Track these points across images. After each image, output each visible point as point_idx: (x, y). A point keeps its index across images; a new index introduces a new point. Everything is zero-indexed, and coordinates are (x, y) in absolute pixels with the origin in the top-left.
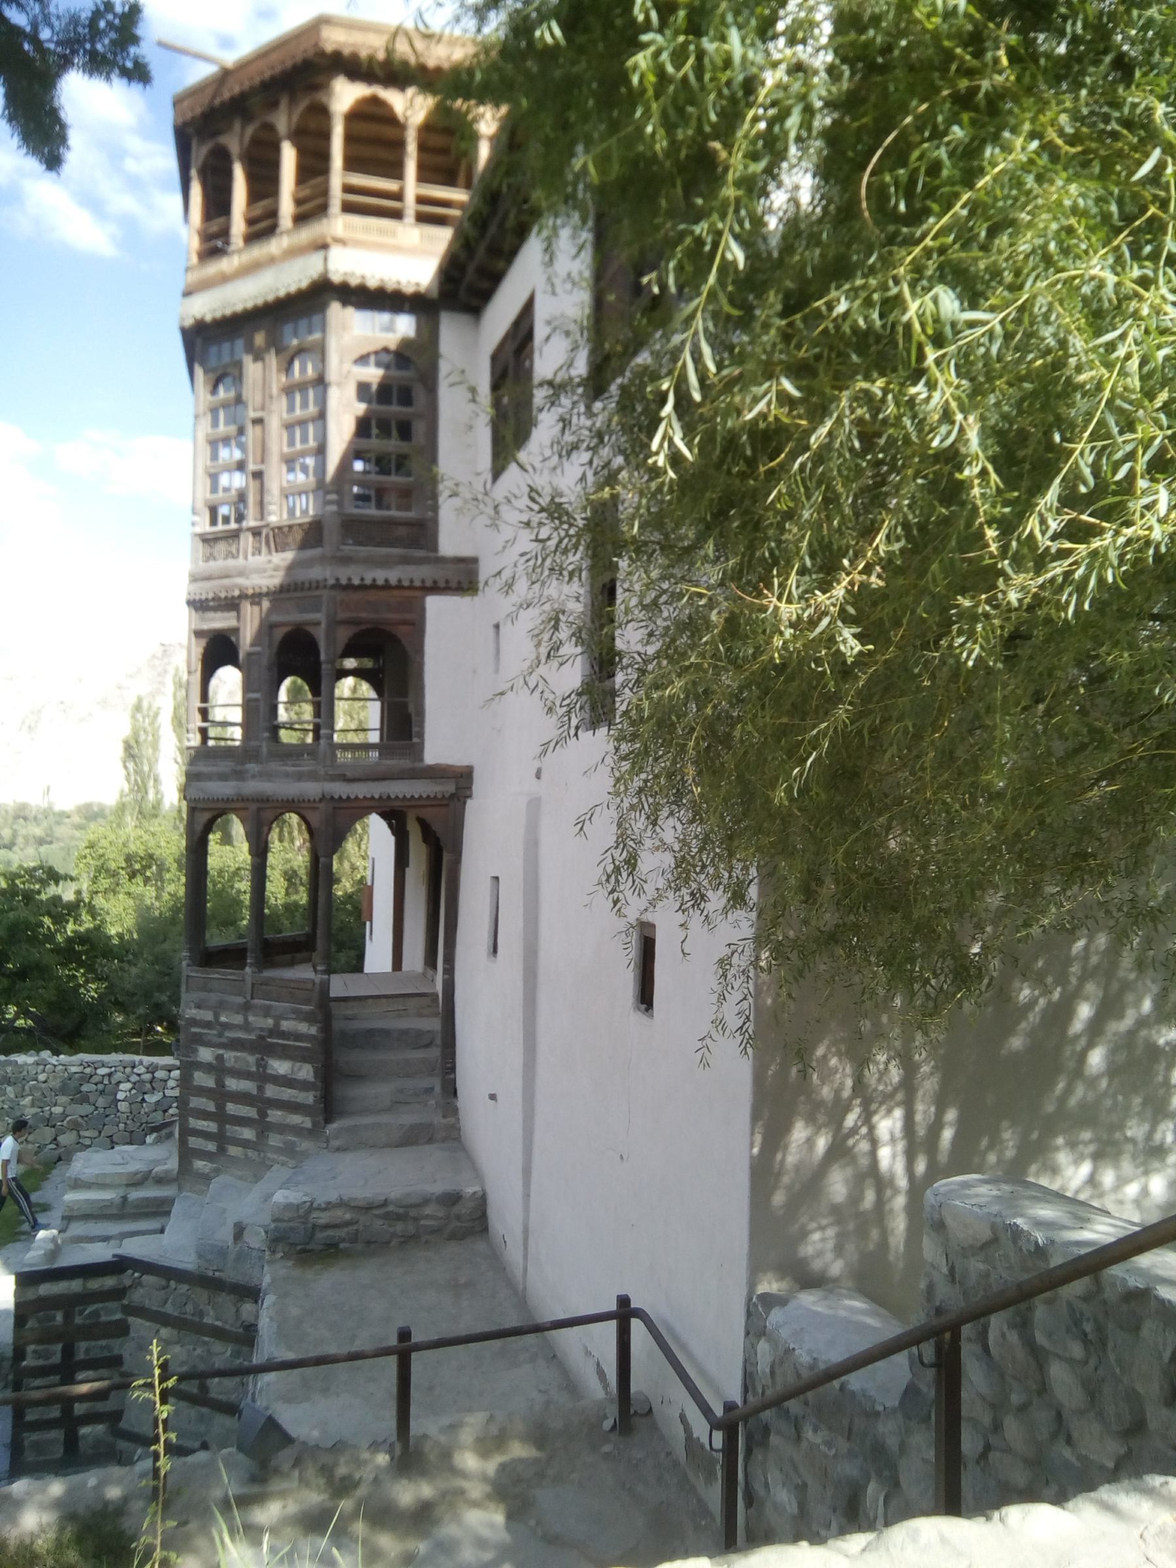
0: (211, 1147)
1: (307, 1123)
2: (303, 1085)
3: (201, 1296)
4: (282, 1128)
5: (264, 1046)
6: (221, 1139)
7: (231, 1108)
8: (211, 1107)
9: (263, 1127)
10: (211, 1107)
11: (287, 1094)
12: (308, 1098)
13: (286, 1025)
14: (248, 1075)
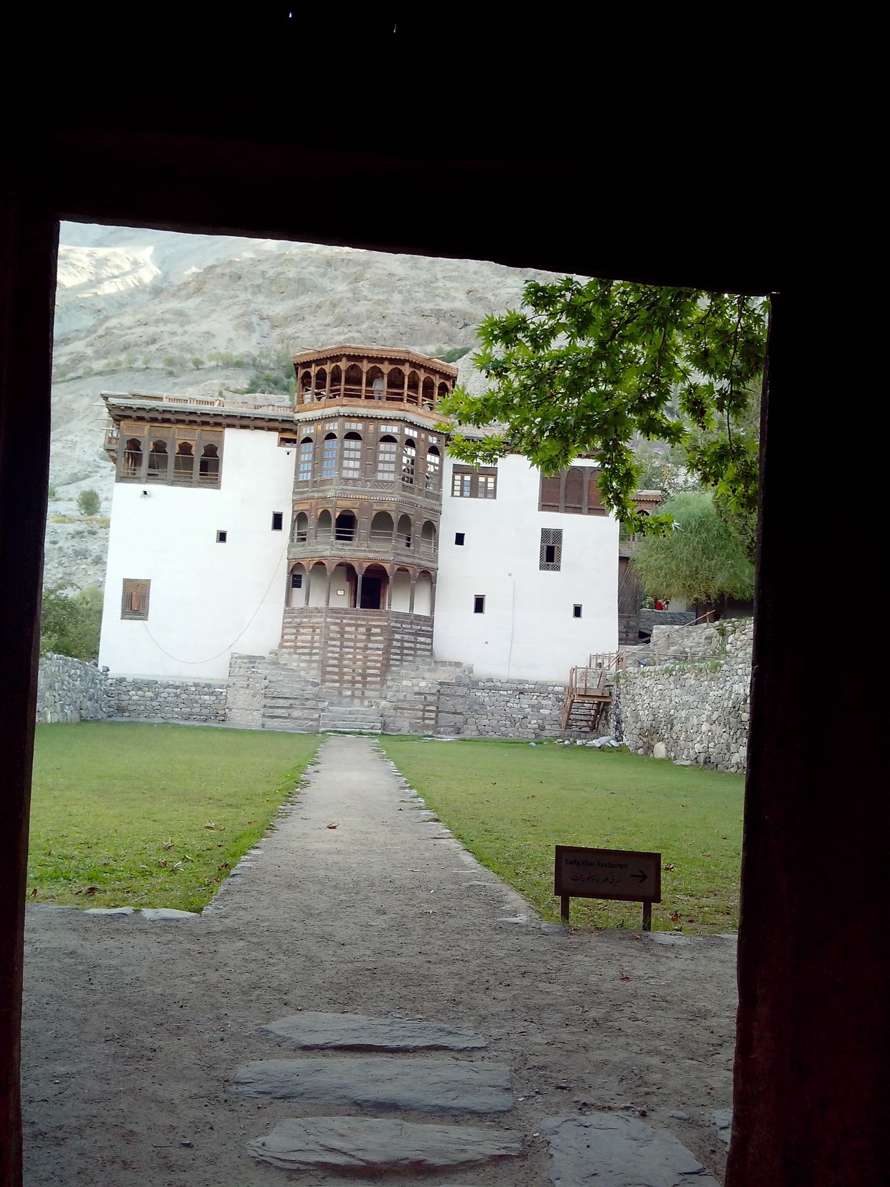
1: (429, 654)
2: (428, 644)
4: (421, 656)
5: (416, 634)
6: (401, 660)
9: (415, 656)
11: (423, 646)
12: (429, 647)
13: (423, 628)
14: (411, 642)
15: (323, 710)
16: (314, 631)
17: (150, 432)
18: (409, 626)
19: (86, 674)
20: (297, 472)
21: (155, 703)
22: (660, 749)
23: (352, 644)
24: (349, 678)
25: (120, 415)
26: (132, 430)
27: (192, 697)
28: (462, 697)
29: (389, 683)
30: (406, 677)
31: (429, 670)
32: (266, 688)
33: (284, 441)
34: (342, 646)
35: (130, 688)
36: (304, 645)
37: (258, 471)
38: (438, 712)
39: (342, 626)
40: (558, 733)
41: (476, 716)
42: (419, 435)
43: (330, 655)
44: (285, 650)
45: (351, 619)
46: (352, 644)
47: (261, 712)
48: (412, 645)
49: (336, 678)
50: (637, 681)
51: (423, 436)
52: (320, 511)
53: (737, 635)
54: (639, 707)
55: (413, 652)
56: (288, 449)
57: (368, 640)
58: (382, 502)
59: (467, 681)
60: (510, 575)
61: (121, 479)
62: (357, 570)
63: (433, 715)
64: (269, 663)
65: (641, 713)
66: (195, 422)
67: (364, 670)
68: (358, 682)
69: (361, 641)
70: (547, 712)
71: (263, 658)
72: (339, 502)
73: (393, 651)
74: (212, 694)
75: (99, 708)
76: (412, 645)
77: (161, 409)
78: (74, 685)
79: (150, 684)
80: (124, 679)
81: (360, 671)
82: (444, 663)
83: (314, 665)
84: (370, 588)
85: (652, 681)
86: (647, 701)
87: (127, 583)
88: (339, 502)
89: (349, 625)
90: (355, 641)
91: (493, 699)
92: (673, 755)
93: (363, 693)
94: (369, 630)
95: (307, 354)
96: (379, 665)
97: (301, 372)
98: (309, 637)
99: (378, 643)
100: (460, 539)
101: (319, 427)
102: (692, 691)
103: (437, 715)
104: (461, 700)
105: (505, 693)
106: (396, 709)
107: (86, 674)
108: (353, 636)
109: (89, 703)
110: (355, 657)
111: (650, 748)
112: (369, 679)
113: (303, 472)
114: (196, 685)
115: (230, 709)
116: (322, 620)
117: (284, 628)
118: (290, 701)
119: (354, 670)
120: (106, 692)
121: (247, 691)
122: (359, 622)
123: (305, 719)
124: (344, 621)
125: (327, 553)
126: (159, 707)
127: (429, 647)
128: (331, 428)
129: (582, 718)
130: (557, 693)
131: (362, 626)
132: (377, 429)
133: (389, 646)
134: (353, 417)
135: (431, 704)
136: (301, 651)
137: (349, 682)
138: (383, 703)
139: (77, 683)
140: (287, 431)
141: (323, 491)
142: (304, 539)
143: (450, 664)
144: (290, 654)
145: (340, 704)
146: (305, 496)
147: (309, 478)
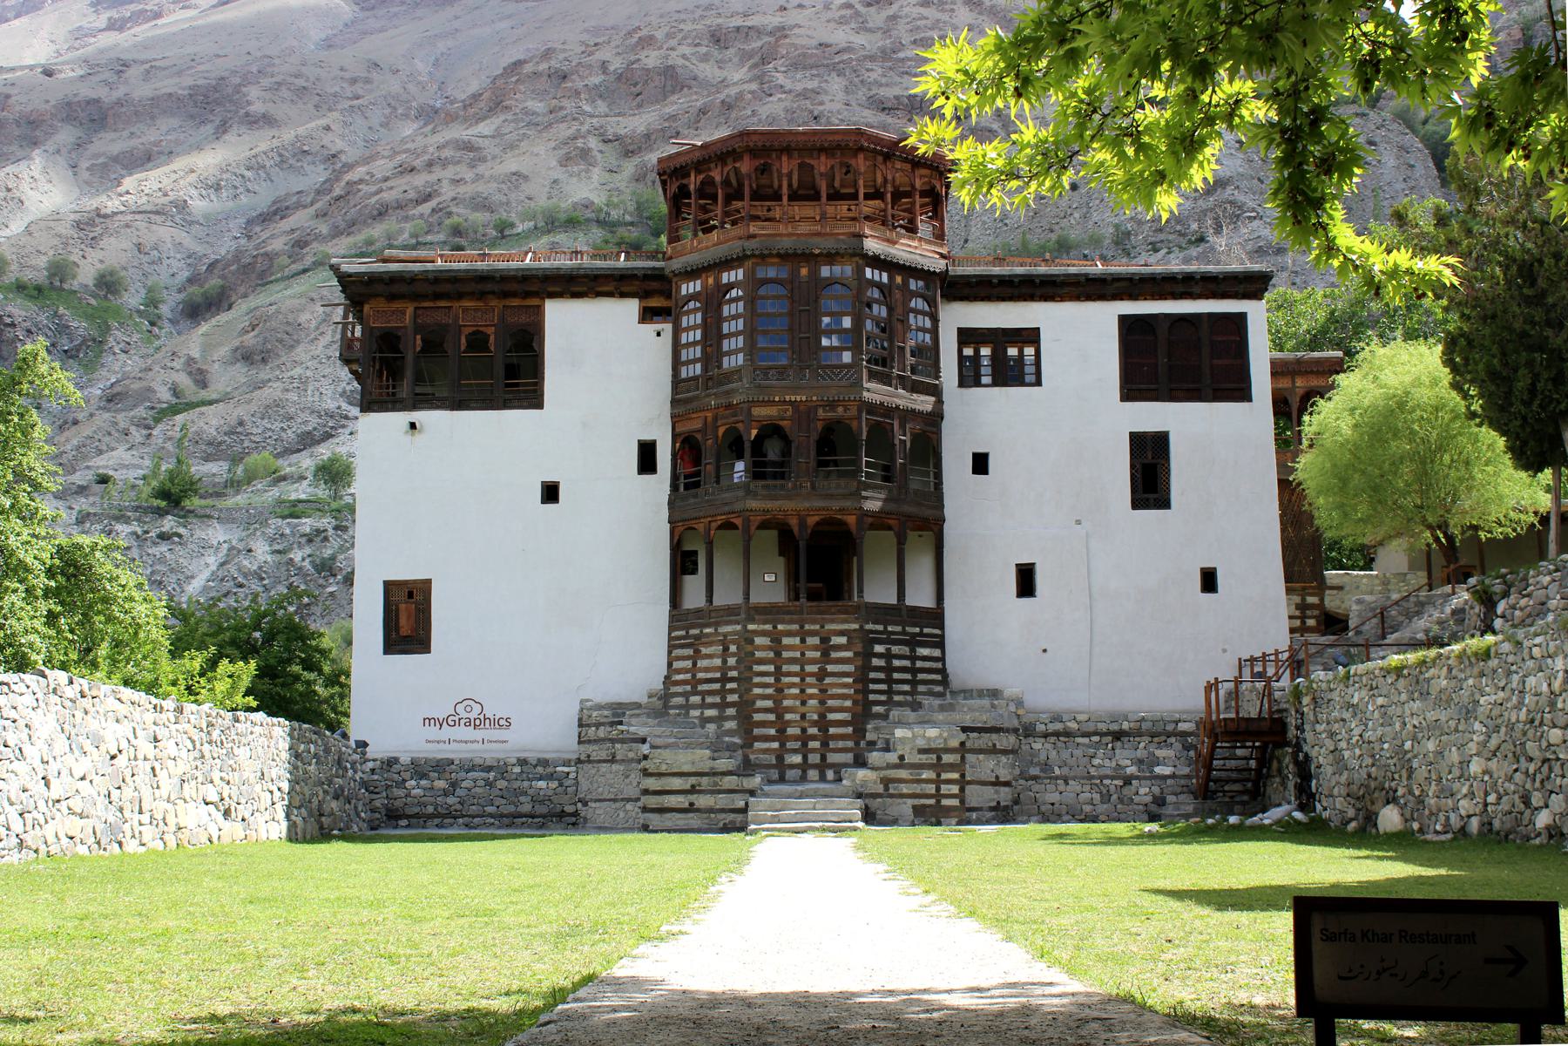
0: (883, 698)
1: (938, 677)
3: (994, 736)
6: (889, 692)
7: (896, 676)
8: (882, 676)
9: (914, 683)
10: (882, 676)
11: (928, 664)
12: (939, 665)
13: (926, 630)
15: (752, 793)
16: (726, 649)
17: (416, 316)
18: (899, 629)
19: (327, 751)
20: (677, 363)
21: (451, 800)
22: (1390, 818)
23: (796, 668)
24: (797, 731)
25: (358, 291)
26: (382, 314)
27: (516, 784)
28: (1005, 752)
29: (870, 736)
30: (901, 723)
31: (942, 708)
32: (646, 757)
33: (647, 315)
34: (778, 674)
35: (407, 775)
36: (710, 675)
37: (608, 369)
38: (963, 783)
39: (776, 639)
40: (1190, 809)
41: (1036, 787)
42: (891, 278)
43: (757, 691)
44: (679, 689)
45: (791, 622)
46: (796, 668)
47: (640, 804)
48: (907, 663)
49: (772, 732)
50: (1335, 696)
51: (899, 279)
52: (721, 431)
53: (1512, 599)
54: (1343, 745)
55: (908, 676)
56: (658, 327)
57: (826, 657)
58: (832, 405)
59: (1015, 723)
60: (1078, 522)
61: (369, 404)
62: (796, 530)
63: (955, 789)
64: (648, 716)
65: (1347, 754)
66: (493, 293)
67: (822, 716)
68: (813, 738)
69: (813, 661)
70: (1167, 771)
71: (638, 706)
72: (756, 411)
73: (872, 675)
74: (550, 777)
75: (352, 813)
76: (907, 663)
77: (430, 276)
78: (306, 772)
79: (441, 766)
80: (396, 760)
81: (815, 717)
82: (967, 693)
83: (731, 711)
84: (822, 566)
85: (1364, 693)
86: (1357, 732)
87: (389, 587)
88: (756, 411)
89: (790, 634)
90: (802, 661)
91: (1065, 755)
92: (1416, 826)
93: (823, 758)
94: (825, 640)
95: (678, 154)
96: (848, 703)
97: (673, 188)
98: (718, 662)
99: (843, 667)
100: (980, 464)
101: (711, 281)
102: (1444, 700)
103: (962, 790)
104: (1004, 759)
105: (1085, 740)
106: (886, 782)
107: (327, 751)
108: (798, 654)
109: (334, 805)
110: (803, 691)
111: (1370, 819)
112: (832, 731)
113: (688, 362)
114: (523, 762)
115: (585, 804)
116: (739, 627)
117: (671, 648)
118: (693, 780)
119: (803, 716)
120: (364, 784)
121: (615, 767)
122: (807, 627)
123: (723, 811)
124: (780, 627)
125: (738, 506)
126: (458, 807)
127: (939, 665)
128: (733, 279)
129: (1234, 775)
130: (1184, 734)
131: (813, 633)
132: (814, 273)
133: (866, 668)
134: (771, 255)
135: (951, 767)
136: (705, 687)
137: (795, 738)
138: (861, 773)
139: (312, 768)
140: (654, 294)
141: (728, 393)
142: (697, 485)
143: (981, 693)
144: (686, 695)
145: (782, 779)
146: (695, 405)
147: (698, 371)
